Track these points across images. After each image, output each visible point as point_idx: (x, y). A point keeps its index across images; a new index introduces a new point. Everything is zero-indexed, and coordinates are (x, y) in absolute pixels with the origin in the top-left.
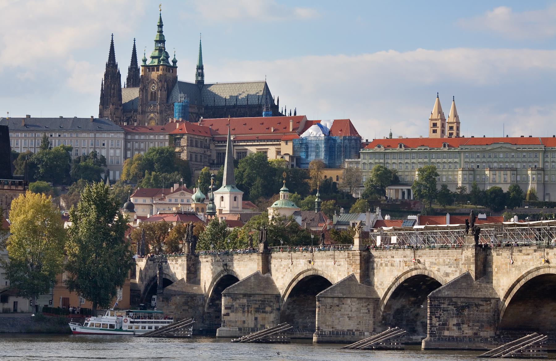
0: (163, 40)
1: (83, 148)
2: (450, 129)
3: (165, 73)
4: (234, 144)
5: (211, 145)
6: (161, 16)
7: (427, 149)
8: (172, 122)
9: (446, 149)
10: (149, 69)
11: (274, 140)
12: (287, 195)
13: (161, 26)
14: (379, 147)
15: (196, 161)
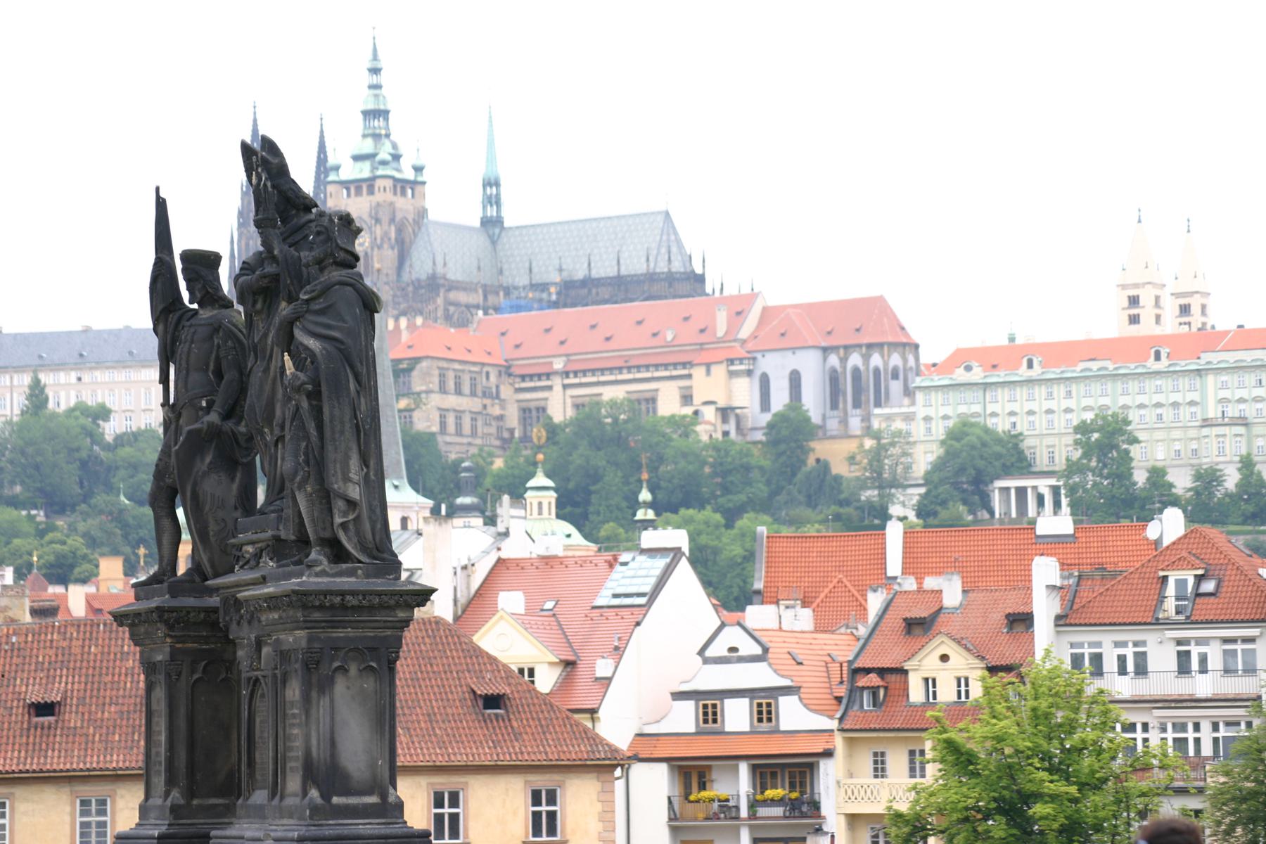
0: (382, 107)
1: (144, 411)
2: (1181, 312)
3: (389, 196)
4: (567, 381)
5: (502, 388)
6: (374, 44)
7: (1106, 369)
8: (397, 327)
9: (1163, 364)
10: (348, 189)
11: (675, 365)
12: (550, 503)
13: (375, 71)
14: (968, 369)
15: (459, 433)
